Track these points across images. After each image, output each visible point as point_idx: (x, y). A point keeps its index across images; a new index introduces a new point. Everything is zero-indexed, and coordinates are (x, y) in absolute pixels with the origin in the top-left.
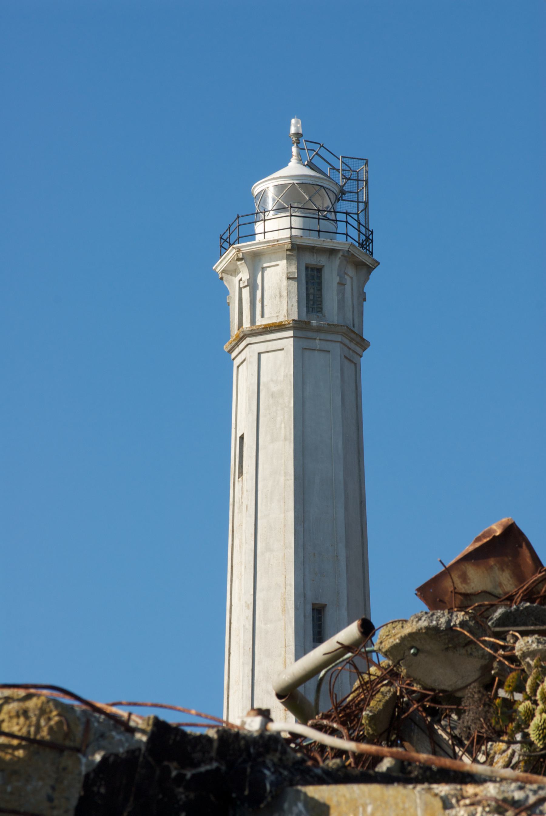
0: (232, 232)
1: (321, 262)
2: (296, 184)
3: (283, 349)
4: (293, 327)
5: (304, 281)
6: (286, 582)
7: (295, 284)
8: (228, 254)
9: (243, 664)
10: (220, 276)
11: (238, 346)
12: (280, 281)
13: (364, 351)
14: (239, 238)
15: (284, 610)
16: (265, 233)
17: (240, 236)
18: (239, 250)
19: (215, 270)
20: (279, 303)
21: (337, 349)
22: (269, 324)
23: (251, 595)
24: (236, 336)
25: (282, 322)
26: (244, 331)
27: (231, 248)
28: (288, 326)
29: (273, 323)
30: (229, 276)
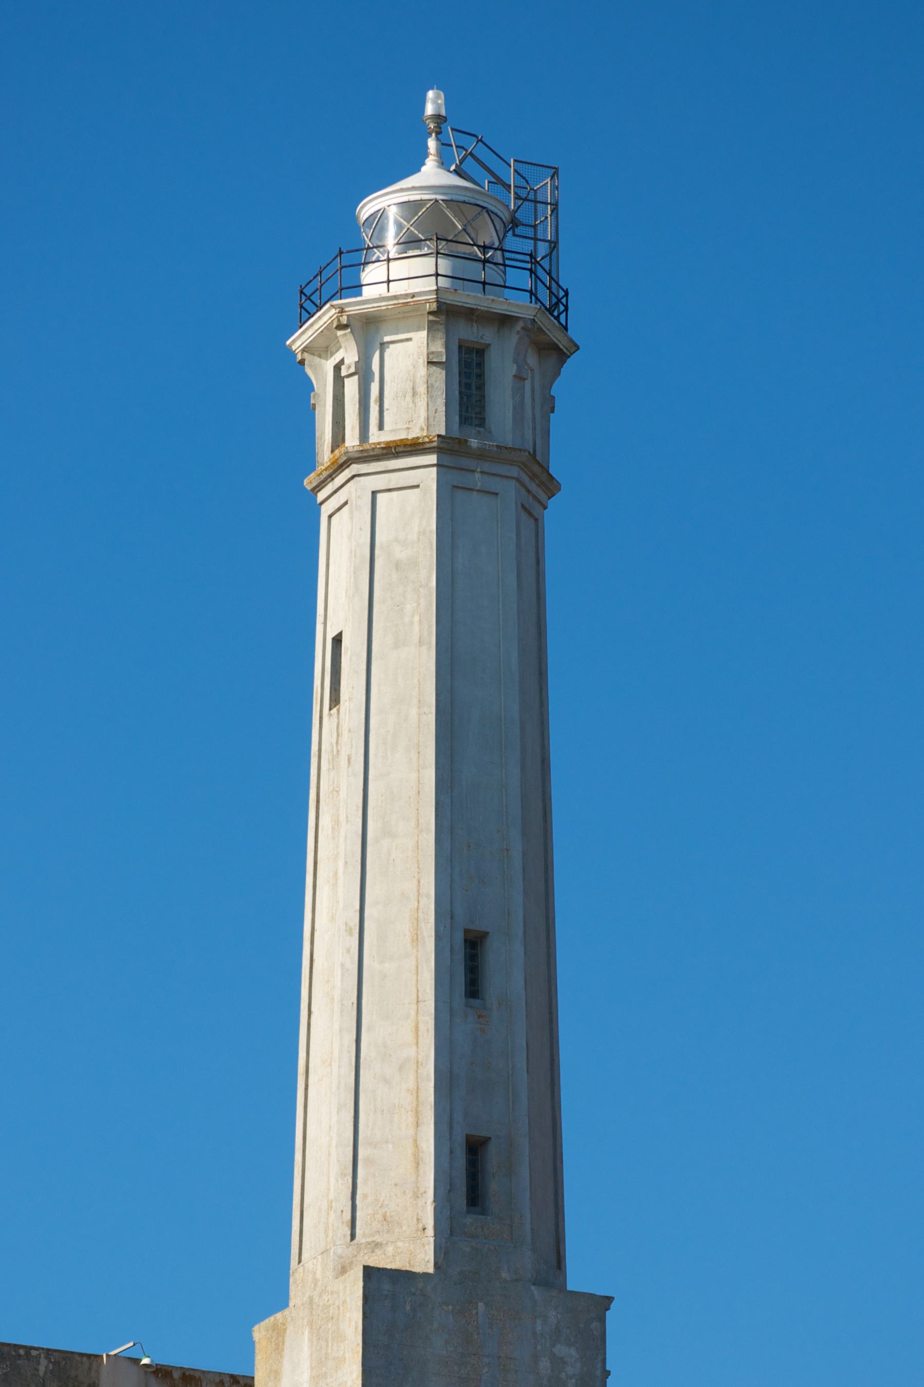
0: (324, 283)
1: (485, 337)
2: (441, 202)
3: (418, 486)
4: (438, 448)
5: (456, 370)
6: (421, 891)
7: (441, 373)
8: (320, 318)
9: (341, 1030)
10: (299, 357)
11: (333, 479)
12: (414, 367)
13: (550, 498)
15: (416, 939)
16: (389, 281)
17: (343, 286)
18: (342, 311)
19: (290, 346)
20: (411, 405)
21: (509, 490)
22: (394, 441)
23: (356, 911)
24: (331, 462)
25: (418, 438)
26: (348, 452)
27: (328, 306)
28: (428, 446)
29: (401, 440)
30: (316, 357)
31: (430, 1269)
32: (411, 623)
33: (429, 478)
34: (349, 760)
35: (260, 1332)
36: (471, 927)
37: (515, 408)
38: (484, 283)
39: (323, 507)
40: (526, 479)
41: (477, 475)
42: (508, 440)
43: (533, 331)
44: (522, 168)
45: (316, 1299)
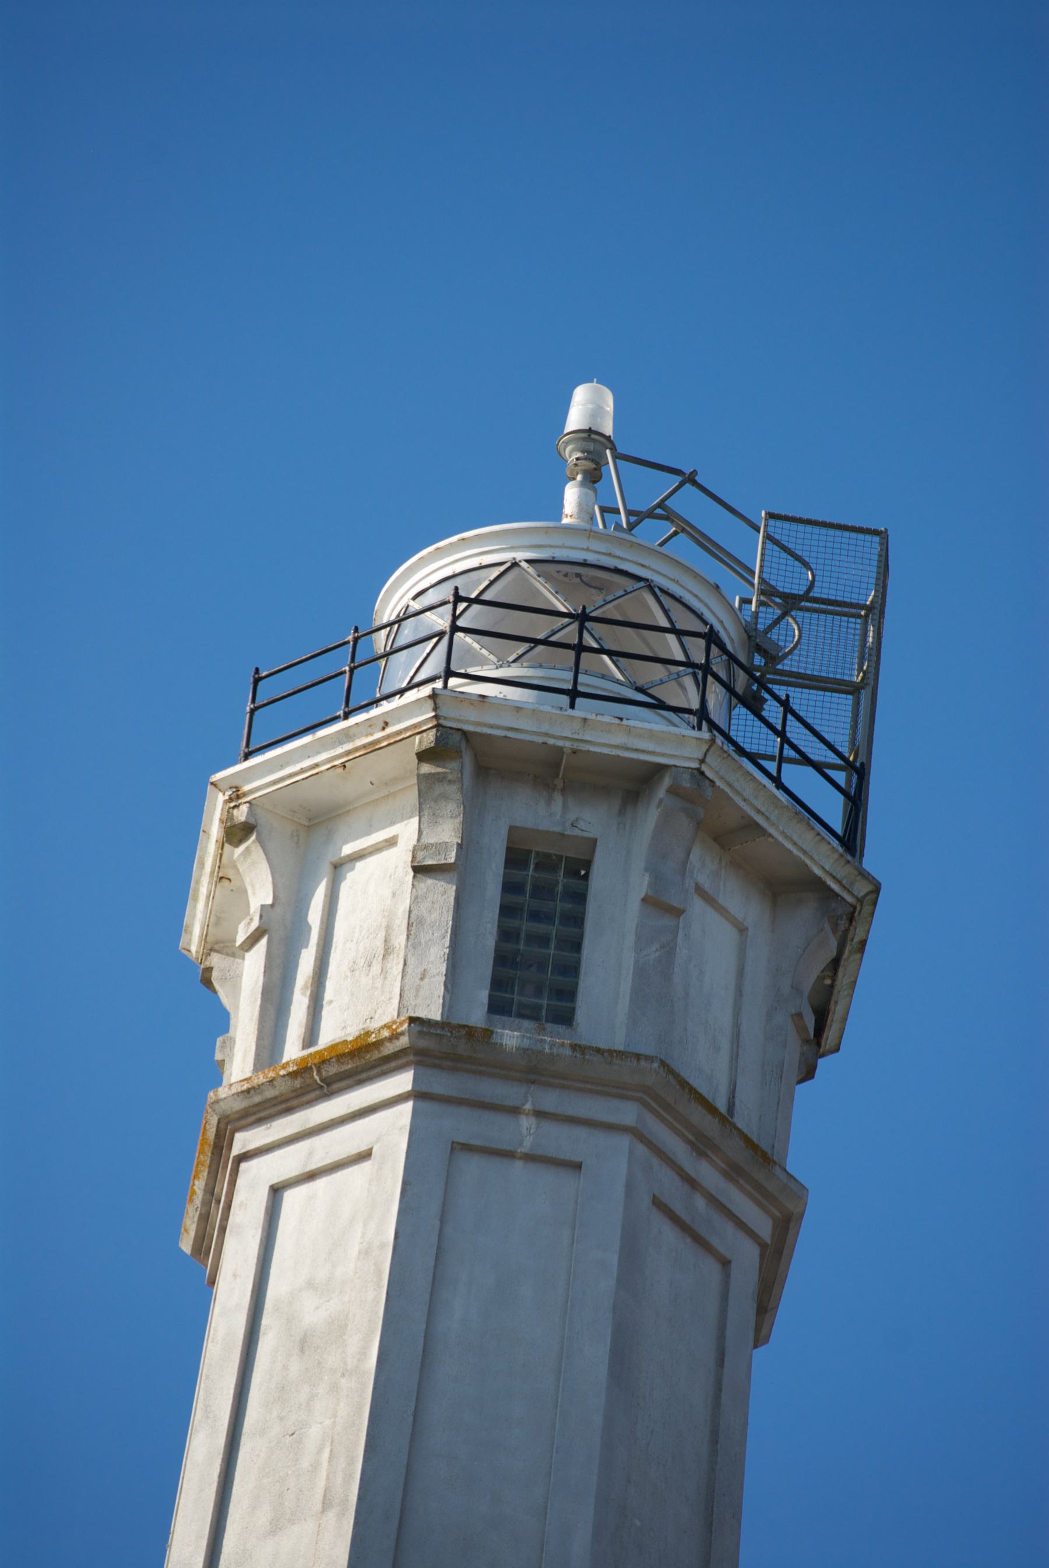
1: (582, 825)
25: (368, 1034)
28: (389, 1049)
32: (315, 1467)
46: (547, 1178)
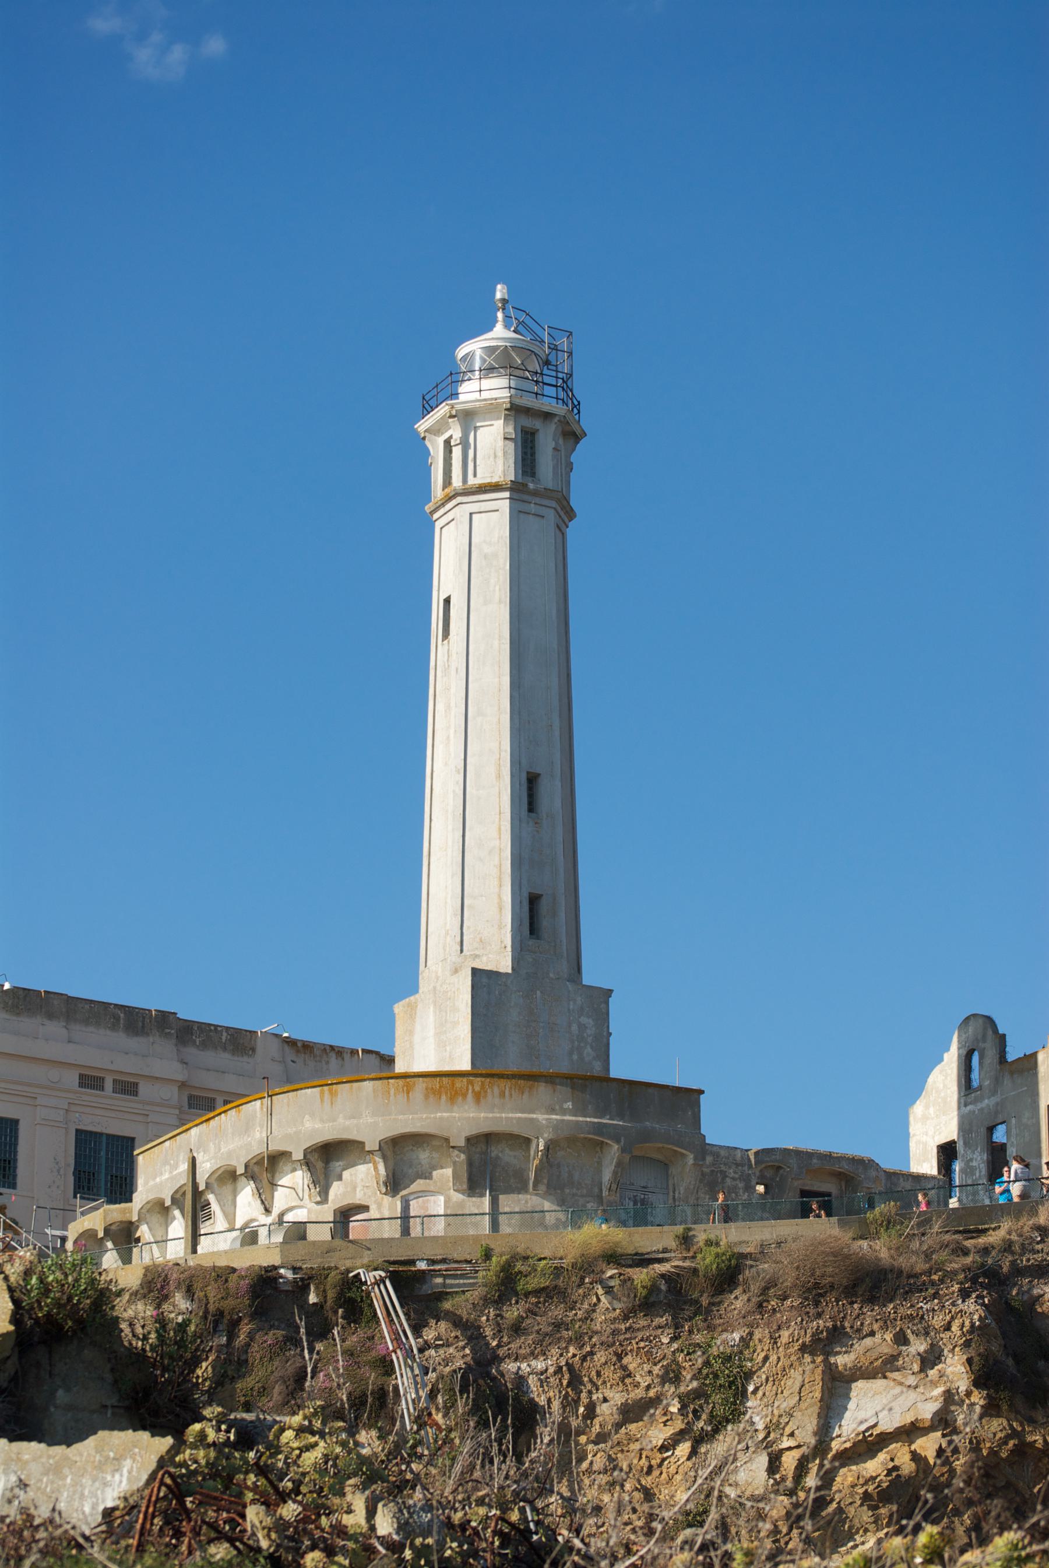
3: (498, 510)
5: (520, 444)
9: (453, 829)
10: (422, 435)
14: (452, 395)
15: (499, 776)
16: (480, 391)
18: (453, 407)
21: (551, 515)
27: (444, 404)
31: (510, 971)
32: (494, 591)
33: (504, 506)
34: (457, 669)
35: (399, 1008)
36: (530, 770)
37: (554, 467)
38: (537, 394)
39: (437, 523)
40: (559, 509)
41: (532, 505)
42: (550, 485)
43: (564, 422)
44: (554, 333)
45: (438, 988)
46: (537, 519)
